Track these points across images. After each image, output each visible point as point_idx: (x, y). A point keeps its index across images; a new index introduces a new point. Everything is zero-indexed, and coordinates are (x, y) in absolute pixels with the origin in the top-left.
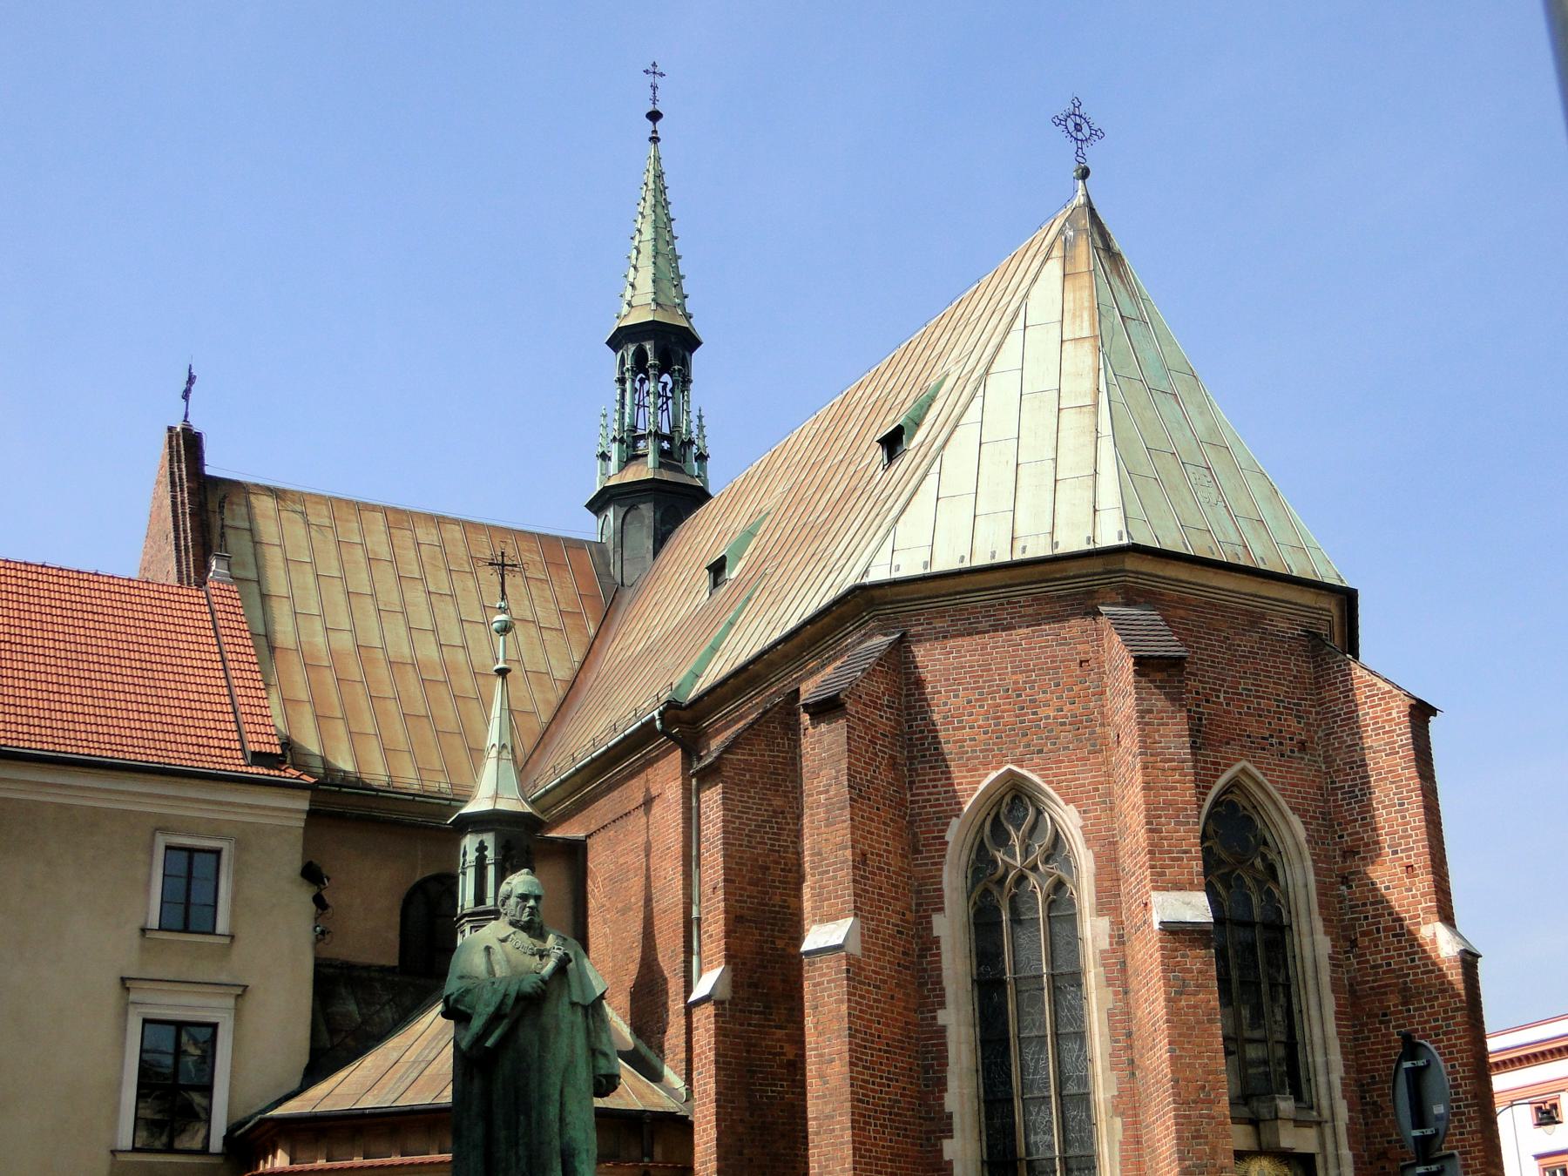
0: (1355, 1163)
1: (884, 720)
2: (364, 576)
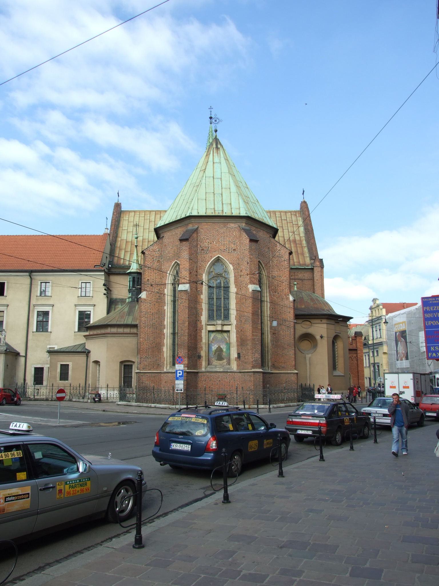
0: (237, 332)
1: (157, 254)
2: (148, 225)
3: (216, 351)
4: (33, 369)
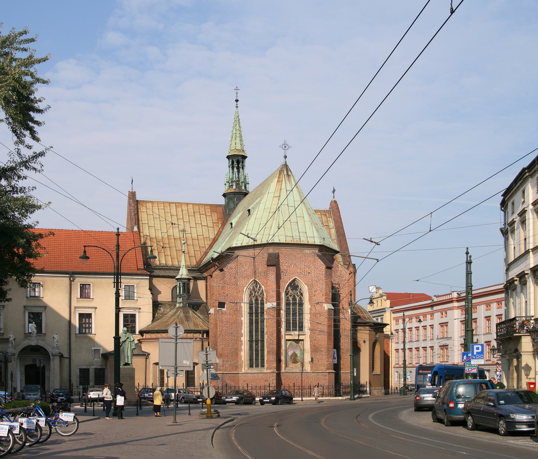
3: (292, 356)
4: (78, 371)
